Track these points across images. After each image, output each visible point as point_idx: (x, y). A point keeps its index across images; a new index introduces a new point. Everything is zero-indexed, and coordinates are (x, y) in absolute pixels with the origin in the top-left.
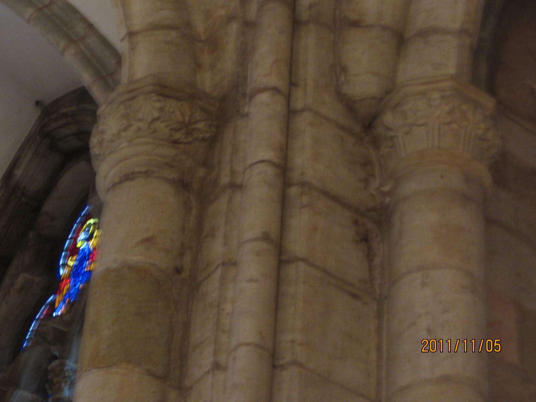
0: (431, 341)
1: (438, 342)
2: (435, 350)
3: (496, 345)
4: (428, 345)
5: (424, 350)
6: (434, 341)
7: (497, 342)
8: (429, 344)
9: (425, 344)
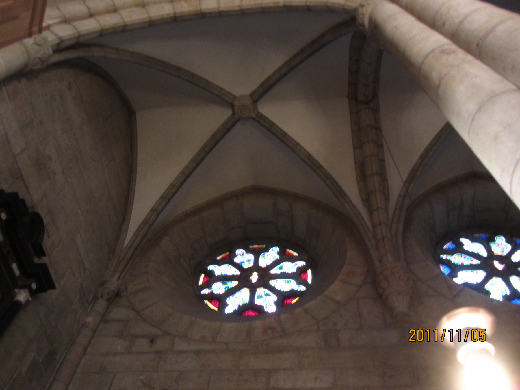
0: (418, 331)
1: (425, 332)
2: (422, 340)
3: (481, 335)
4: (415, 334)
5: (412, 339)
6: (421, 331)
7: (482, 332)
8: (416, 334)
9: (412, 334)
